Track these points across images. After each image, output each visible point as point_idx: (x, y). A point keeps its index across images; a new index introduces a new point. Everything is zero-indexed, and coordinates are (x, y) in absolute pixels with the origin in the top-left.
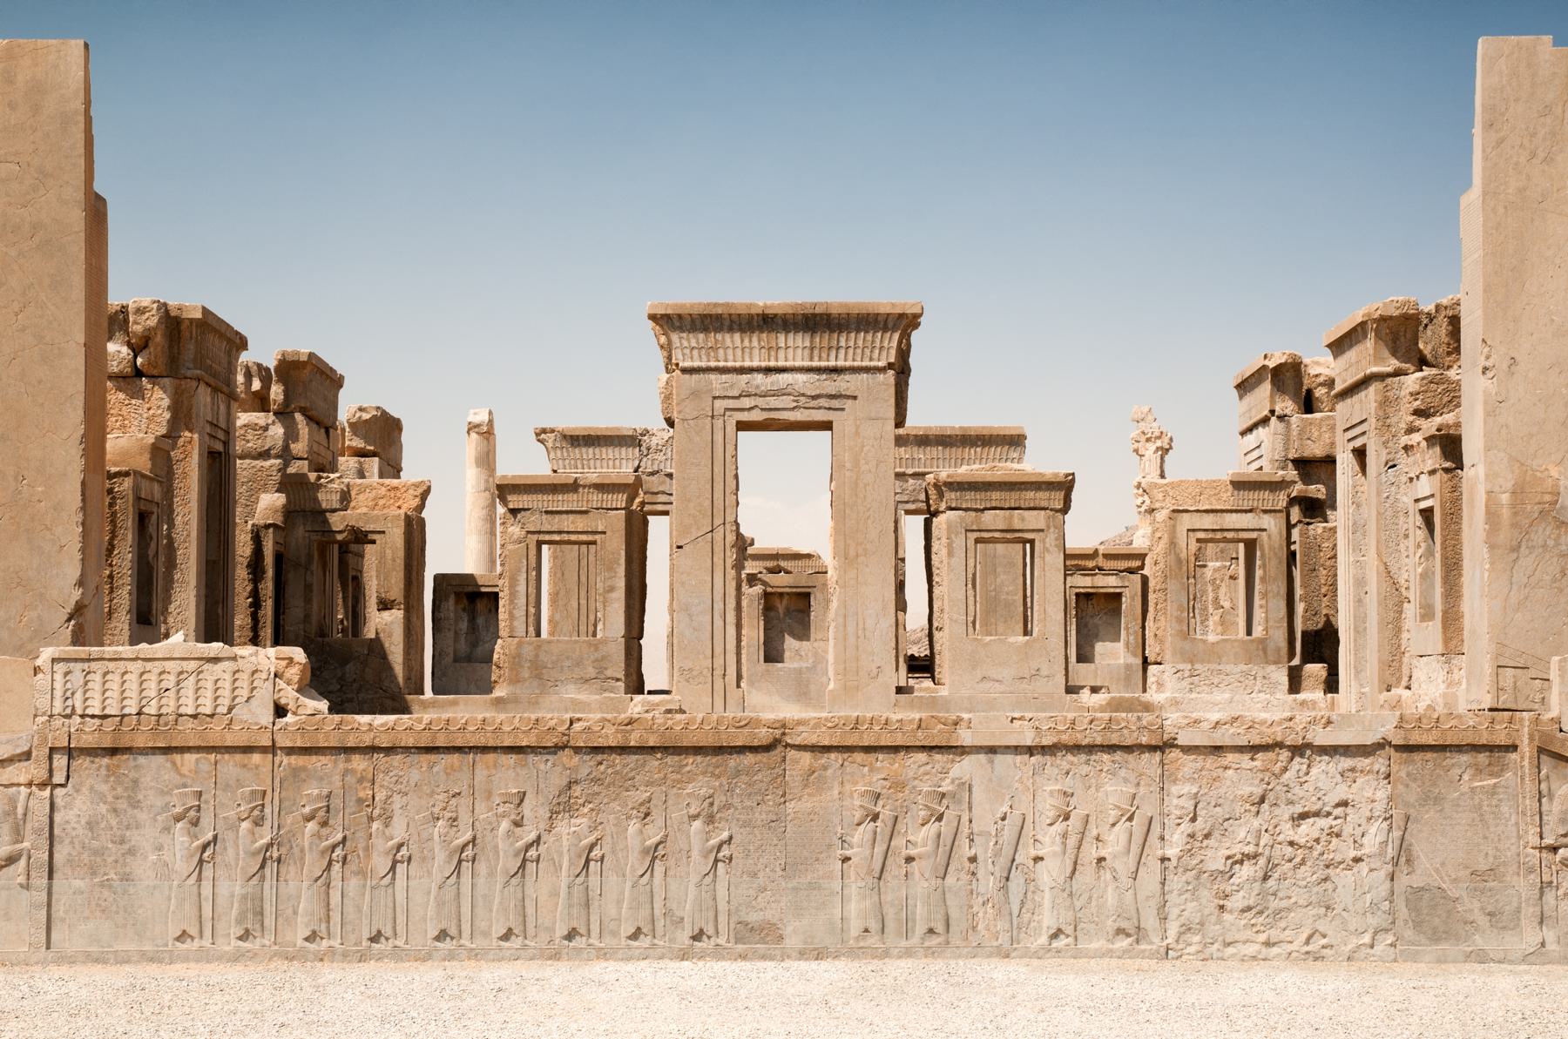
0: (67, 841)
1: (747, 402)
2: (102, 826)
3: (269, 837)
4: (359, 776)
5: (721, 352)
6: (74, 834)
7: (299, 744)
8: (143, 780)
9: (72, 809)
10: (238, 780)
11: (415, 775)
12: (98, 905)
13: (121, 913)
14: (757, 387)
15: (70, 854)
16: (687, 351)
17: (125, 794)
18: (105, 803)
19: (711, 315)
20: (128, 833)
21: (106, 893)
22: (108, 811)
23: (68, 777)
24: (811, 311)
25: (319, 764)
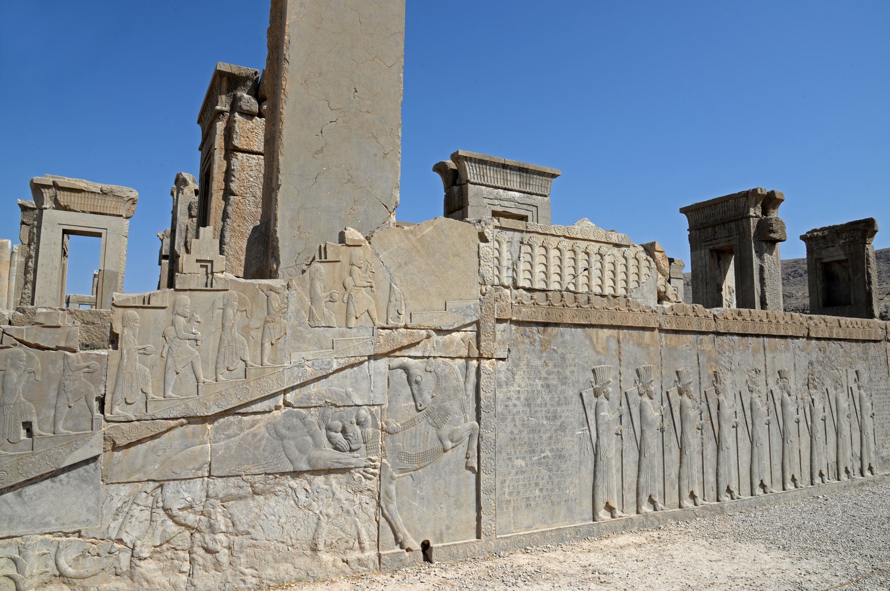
0: (510, 418)
1: (496, 202)
2: (539, 401)
4: (708, 356)
5: (486, 178)
7: (674, 328)
8: (568, 356)
9: (512, 385)
10: (636, 358)
14: (501, 196)
15: (512, 433)
16: (472, 175)
17: (555, 370)
19: (483, 160)
20: (559, 409)
21: (544, 472)
22: (542, 386)
24: (522, 166)
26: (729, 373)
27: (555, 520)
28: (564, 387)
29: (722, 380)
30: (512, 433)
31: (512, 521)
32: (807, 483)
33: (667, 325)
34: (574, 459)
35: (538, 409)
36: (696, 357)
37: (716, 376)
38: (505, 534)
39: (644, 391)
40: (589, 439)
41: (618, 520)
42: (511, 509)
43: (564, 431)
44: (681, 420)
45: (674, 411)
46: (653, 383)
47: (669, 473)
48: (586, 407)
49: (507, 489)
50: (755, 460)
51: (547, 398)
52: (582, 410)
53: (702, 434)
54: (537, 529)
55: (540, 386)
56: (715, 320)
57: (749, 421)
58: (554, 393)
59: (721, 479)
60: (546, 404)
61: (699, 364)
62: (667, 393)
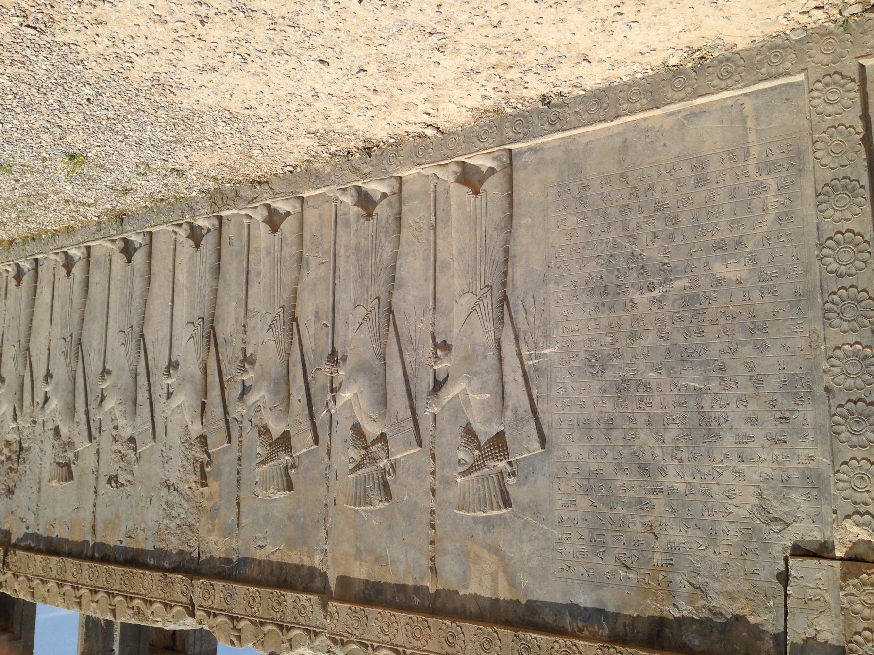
0: (772, 385)
3: (340, 402)
4: (216, 521)
6: (753, 407)
8: (581, 547)
9: (766, 478)
10: (390, 527)
11: (152, 515)
12: (674, 220)
13: (613, 211)
15: (761, 347)
18: (672, 491)
20: (609, 408)
21: (653, 253)
22: (663, 471)
23: (784, 577)
25: (269, 549)
26: (173, 480)
27: (619, 140)
28: (594, 466)
29: (191, 467)
30: (761, 347)
31: (750, 124)
32: (46, 262)
33: (307, 604)
34: (561, 287)
35: (678, 411)
36: (244, 521)
37: (204, 475)
38: (772, 89)
39: (374, 449)
40: (522, 337)
41: (448, 158)
42: (754, 151)
43: (594, 354)
44: (288, 383)
45: (304, 401)
46: (351, 466)
47: (323, 267)
48: (530, 415)
49: (771, 200)
50: (137, 301)
51: (646, 438)
52: (542, 407)
53: (244, 351)
54: (670, 114)
55: (671, 472)
56: (193, 605)
57: (142, 380)
58: (626, 452)
59: (211, 260)
60: (649, 423)
61: (238, 504)
62: (316, 441)
